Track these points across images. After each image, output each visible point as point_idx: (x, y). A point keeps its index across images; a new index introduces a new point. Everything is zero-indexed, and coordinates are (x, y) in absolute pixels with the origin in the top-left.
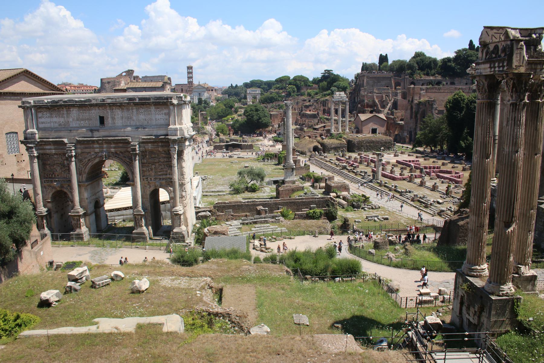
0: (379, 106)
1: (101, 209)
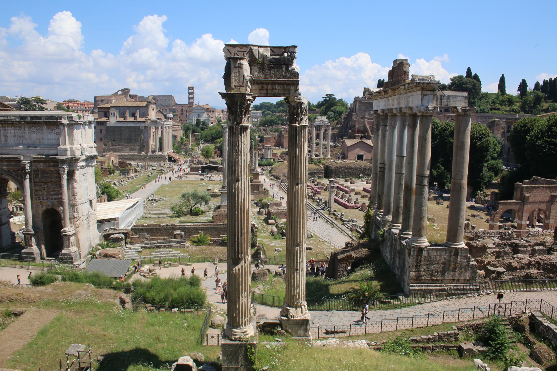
0: (370, 132)
1: (3, 227)
